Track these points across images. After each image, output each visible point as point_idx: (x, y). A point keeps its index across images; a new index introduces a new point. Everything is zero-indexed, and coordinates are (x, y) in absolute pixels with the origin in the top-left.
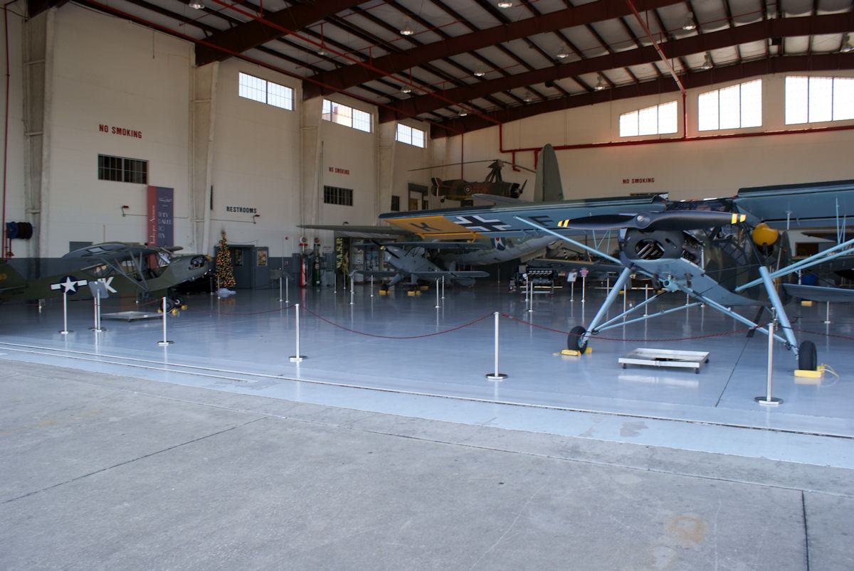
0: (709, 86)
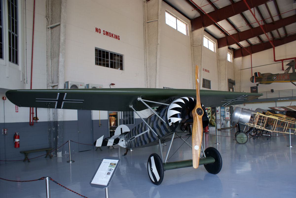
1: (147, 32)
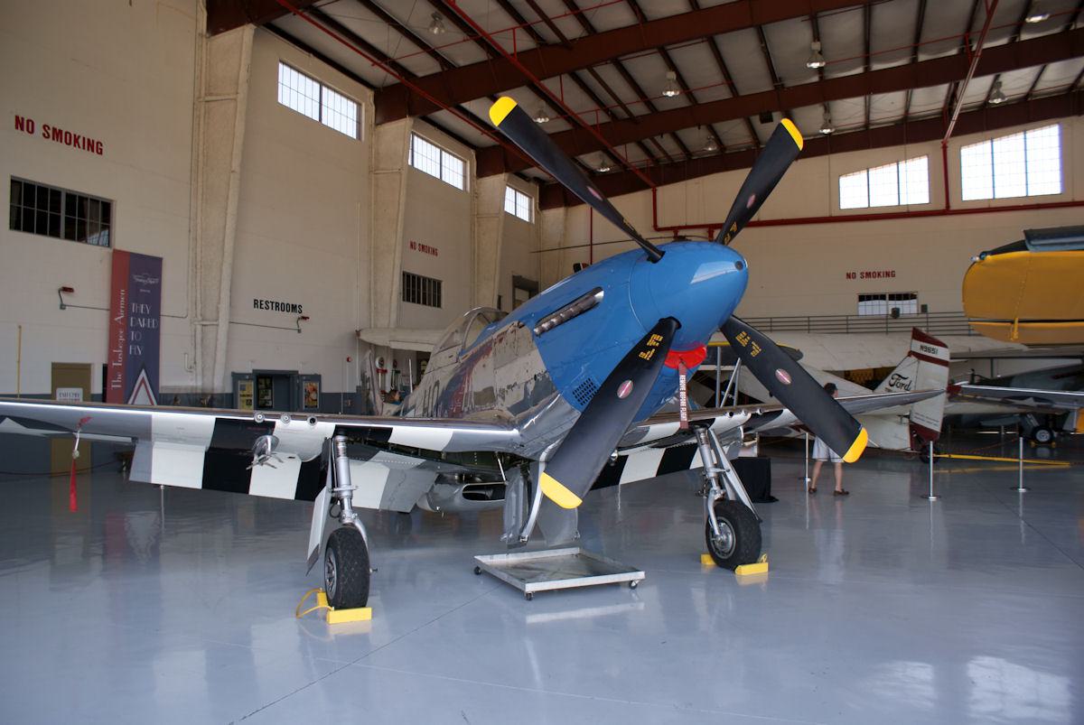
0: (979, 134)
1: (202, 130)
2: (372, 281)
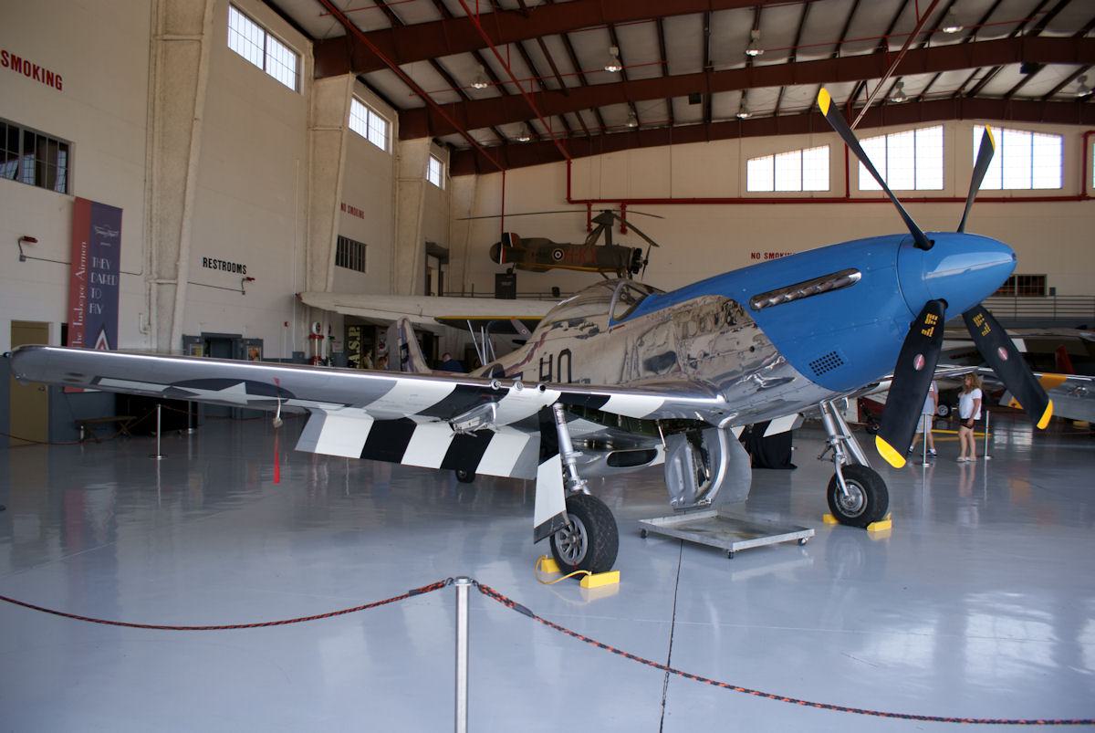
2: (309, 244)
